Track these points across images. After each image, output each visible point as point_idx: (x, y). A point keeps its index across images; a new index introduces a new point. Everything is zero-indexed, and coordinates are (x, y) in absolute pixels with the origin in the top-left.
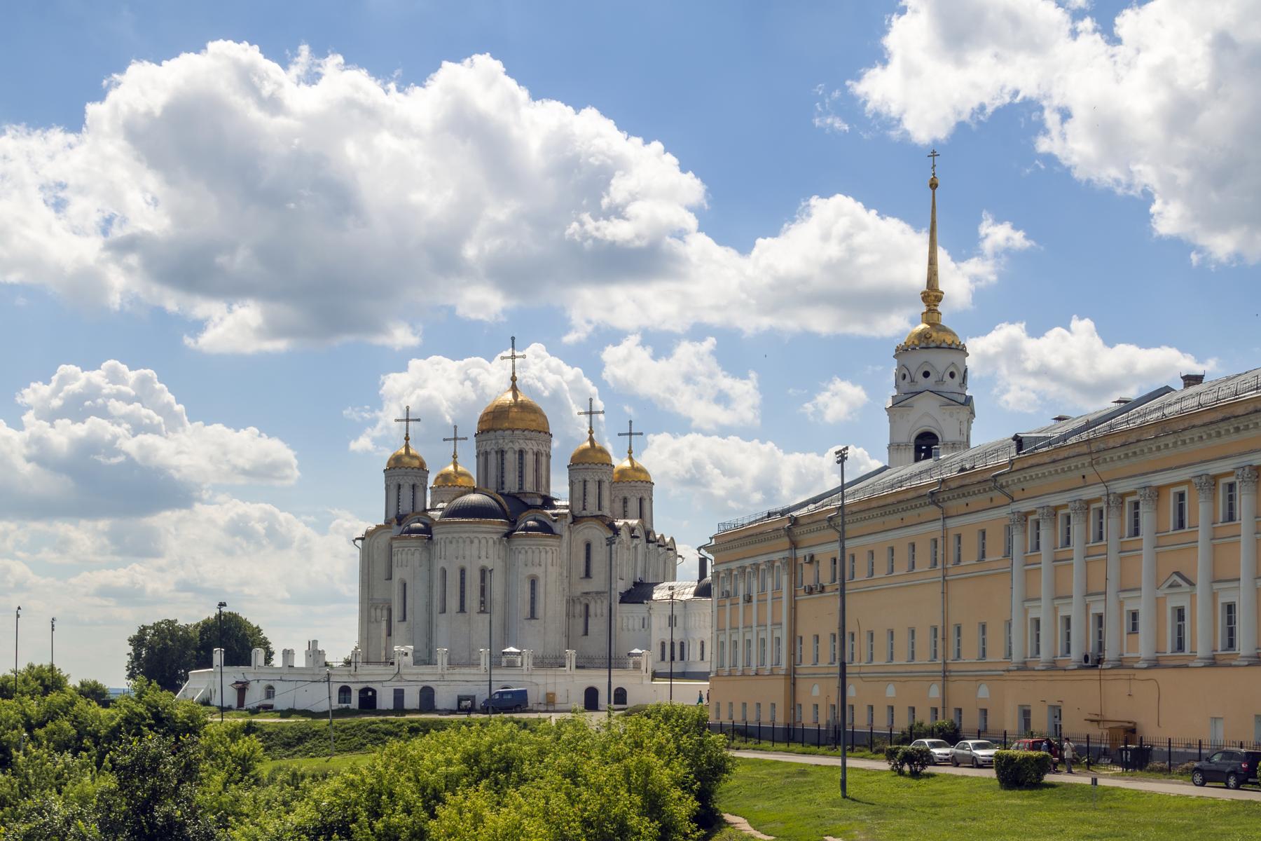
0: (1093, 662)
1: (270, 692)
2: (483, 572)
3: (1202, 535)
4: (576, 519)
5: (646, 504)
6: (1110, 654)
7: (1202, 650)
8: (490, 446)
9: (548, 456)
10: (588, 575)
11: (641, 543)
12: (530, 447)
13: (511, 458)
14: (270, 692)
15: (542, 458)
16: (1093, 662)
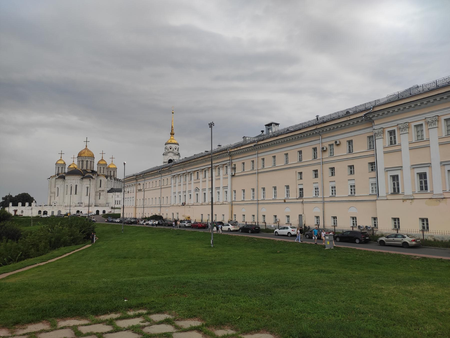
0: (184, 204)
1: (22, 212)
2: (76, 186)
3: (201, 181)
4: (98, 175)
5: (115, 172)
6: (186, 203)
7: (201, 202)
8: (80, 160)
9: (94, 162)
10: (100, 187)
11: (113, 180)
12: (89, 160)
13: (85, 163)
14: (22, 212)
15: (92, 162)
16: (184, 204)
